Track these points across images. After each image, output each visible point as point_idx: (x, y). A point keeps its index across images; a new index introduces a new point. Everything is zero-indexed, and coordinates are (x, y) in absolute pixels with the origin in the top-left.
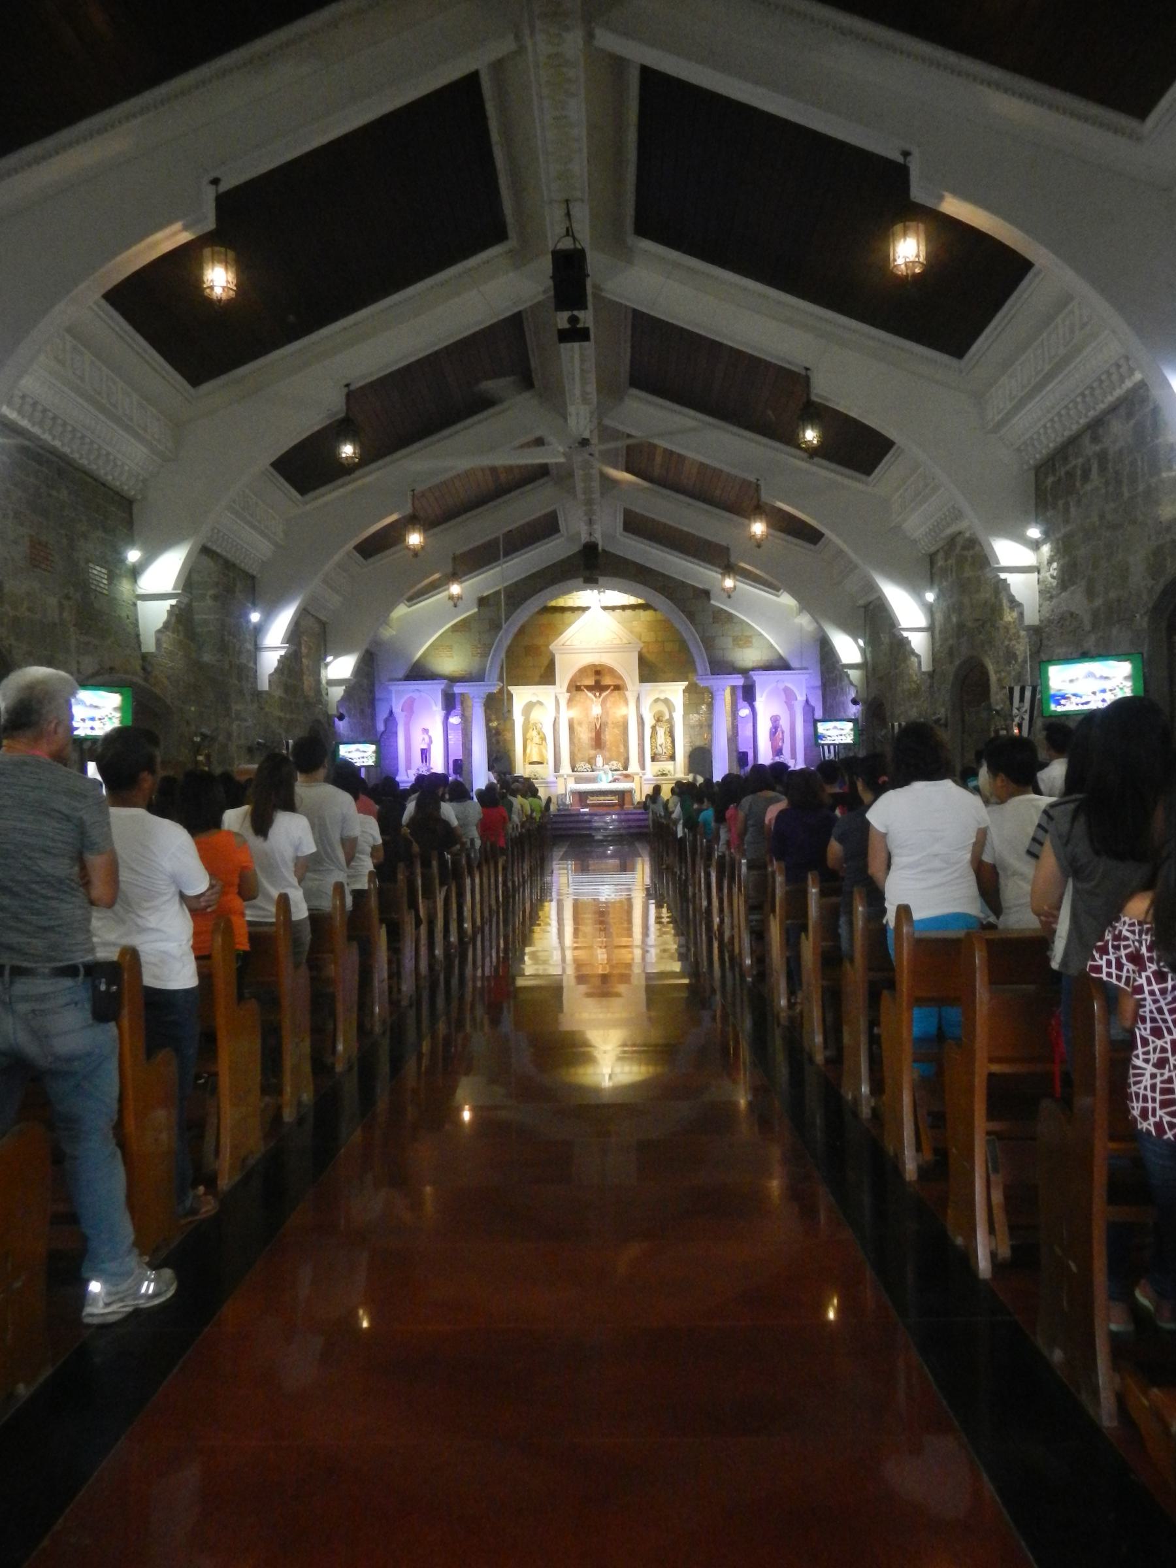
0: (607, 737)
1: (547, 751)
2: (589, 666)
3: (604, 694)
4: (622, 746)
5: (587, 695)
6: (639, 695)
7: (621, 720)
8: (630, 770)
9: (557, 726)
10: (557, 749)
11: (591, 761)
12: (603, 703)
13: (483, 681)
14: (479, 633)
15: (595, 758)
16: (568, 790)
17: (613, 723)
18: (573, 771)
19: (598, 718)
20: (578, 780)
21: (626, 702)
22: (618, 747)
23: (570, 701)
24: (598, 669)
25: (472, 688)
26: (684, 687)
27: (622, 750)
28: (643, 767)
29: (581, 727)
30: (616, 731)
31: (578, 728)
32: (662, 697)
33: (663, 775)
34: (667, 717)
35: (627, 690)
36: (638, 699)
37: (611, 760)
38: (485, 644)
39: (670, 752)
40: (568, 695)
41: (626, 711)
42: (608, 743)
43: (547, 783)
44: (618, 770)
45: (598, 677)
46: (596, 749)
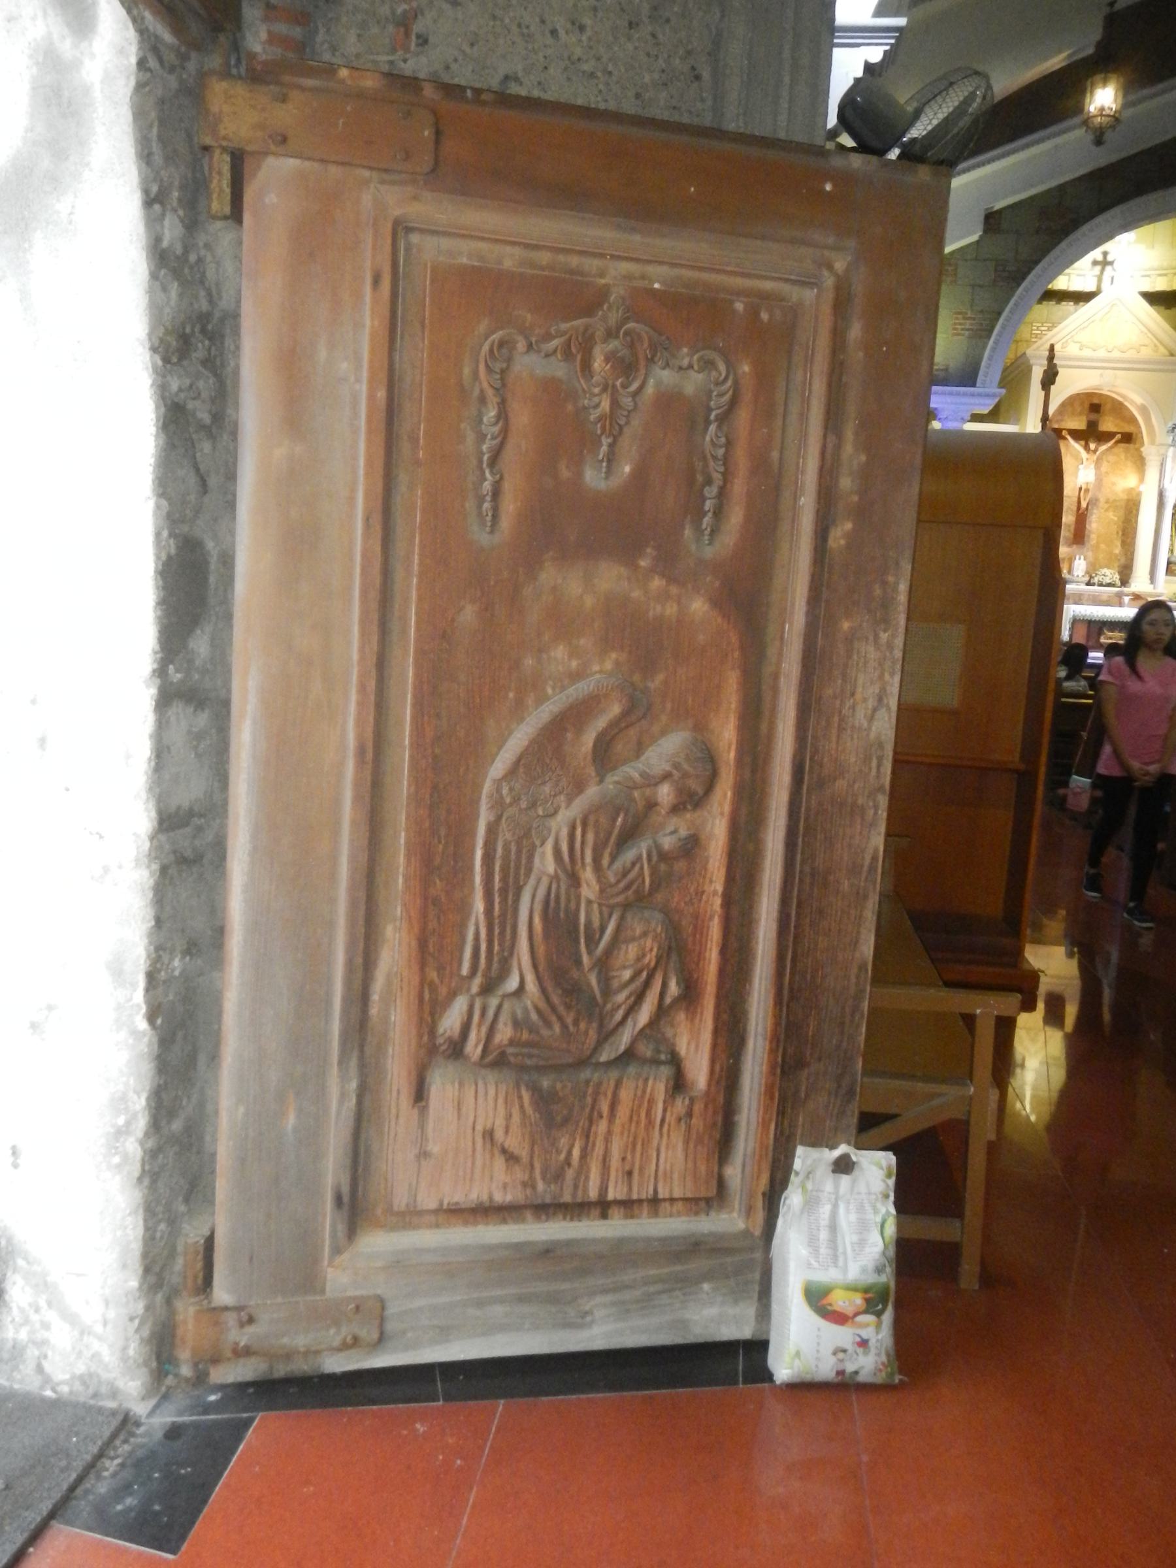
2: (1078, 394)
3: (1103, 448)
4: (1119, 543)
12: (1098, 463)
13: (974, 385)
14: (973, 286)
17: (1107, 502)
21: (1140, 463)
24: (1096, 401)
25: (949, 399)
27: (1117, 551)
30: (1111, 515)
38: (982, 312)
41: (1125, 481)
42: (1093, 536)
45: (1093, 417)
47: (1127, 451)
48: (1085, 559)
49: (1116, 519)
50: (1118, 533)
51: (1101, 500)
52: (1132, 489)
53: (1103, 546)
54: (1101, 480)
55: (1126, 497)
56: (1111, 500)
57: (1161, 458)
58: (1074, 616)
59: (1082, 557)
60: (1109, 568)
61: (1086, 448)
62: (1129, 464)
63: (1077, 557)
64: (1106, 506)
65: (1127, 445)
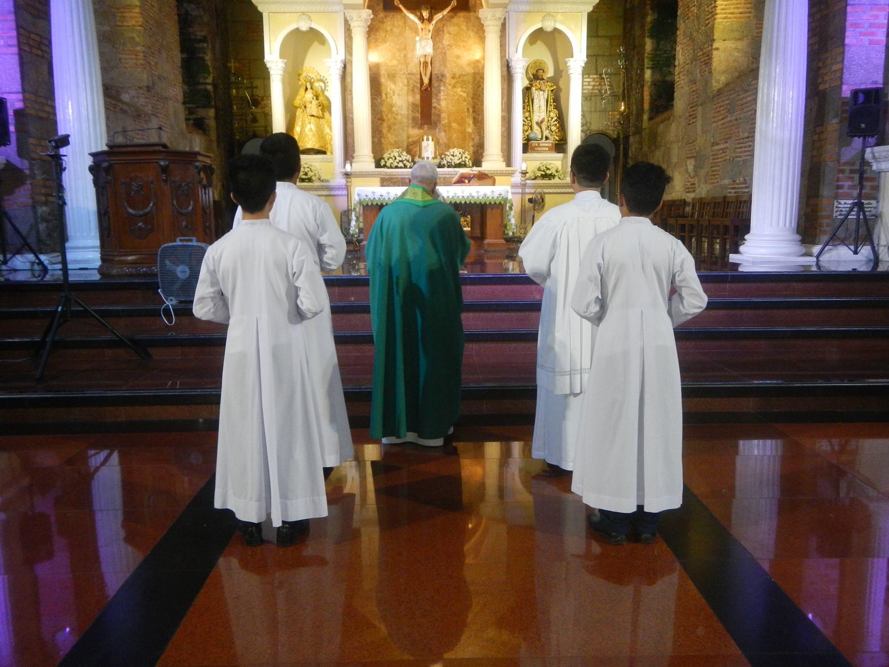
0: (443, 104)
1: (331, 128)
3: (439, 16)
4: (470, 121)
5: (405, 17)
6: (505, 19)
7: (470, 70)
8: (487, 166)
9: (348, 80)
10: (349, 126)
11: (413, 149)
12: (437, 35)
15: (418, 143)
16: (355, 198)
17: (453, 78)
18: (378, 165)
19: (426, 63)
20: (386, 182)
21: (480, 31)
22: (462, 123)
23: (372, 31)
26: (590, 9)
27: (470, 130)
28: (509, 161)
29: (395, 83)
30: (459, 90)
31: (388, 86)
32: (549, 26)
33: (545, 176)
34: (550, 73)
35: (482, 7)
36: (503, 27)
37: (448, 147)
39: (554, 138)
40: (367, 14)
42: (443, 115)
43: (330, 188)
44: (465, 166)
46: (420, 128)
47: (468, 20)
48: (433, 140)
49: (465, 95)
50: (468, 109)
51: (448, 75)
52: (478, 61)
53: (454, 125)
54: (445, 54)
55: (472, 71)
56: (457, 76)
57: (499, 23)
58: (360, 199)
59: (430, 138)
60: (459, 148)
61: (422, 19)
62: (471, 34)
63: (425, 138)
64: (453, 81)
65: (467, 14)
